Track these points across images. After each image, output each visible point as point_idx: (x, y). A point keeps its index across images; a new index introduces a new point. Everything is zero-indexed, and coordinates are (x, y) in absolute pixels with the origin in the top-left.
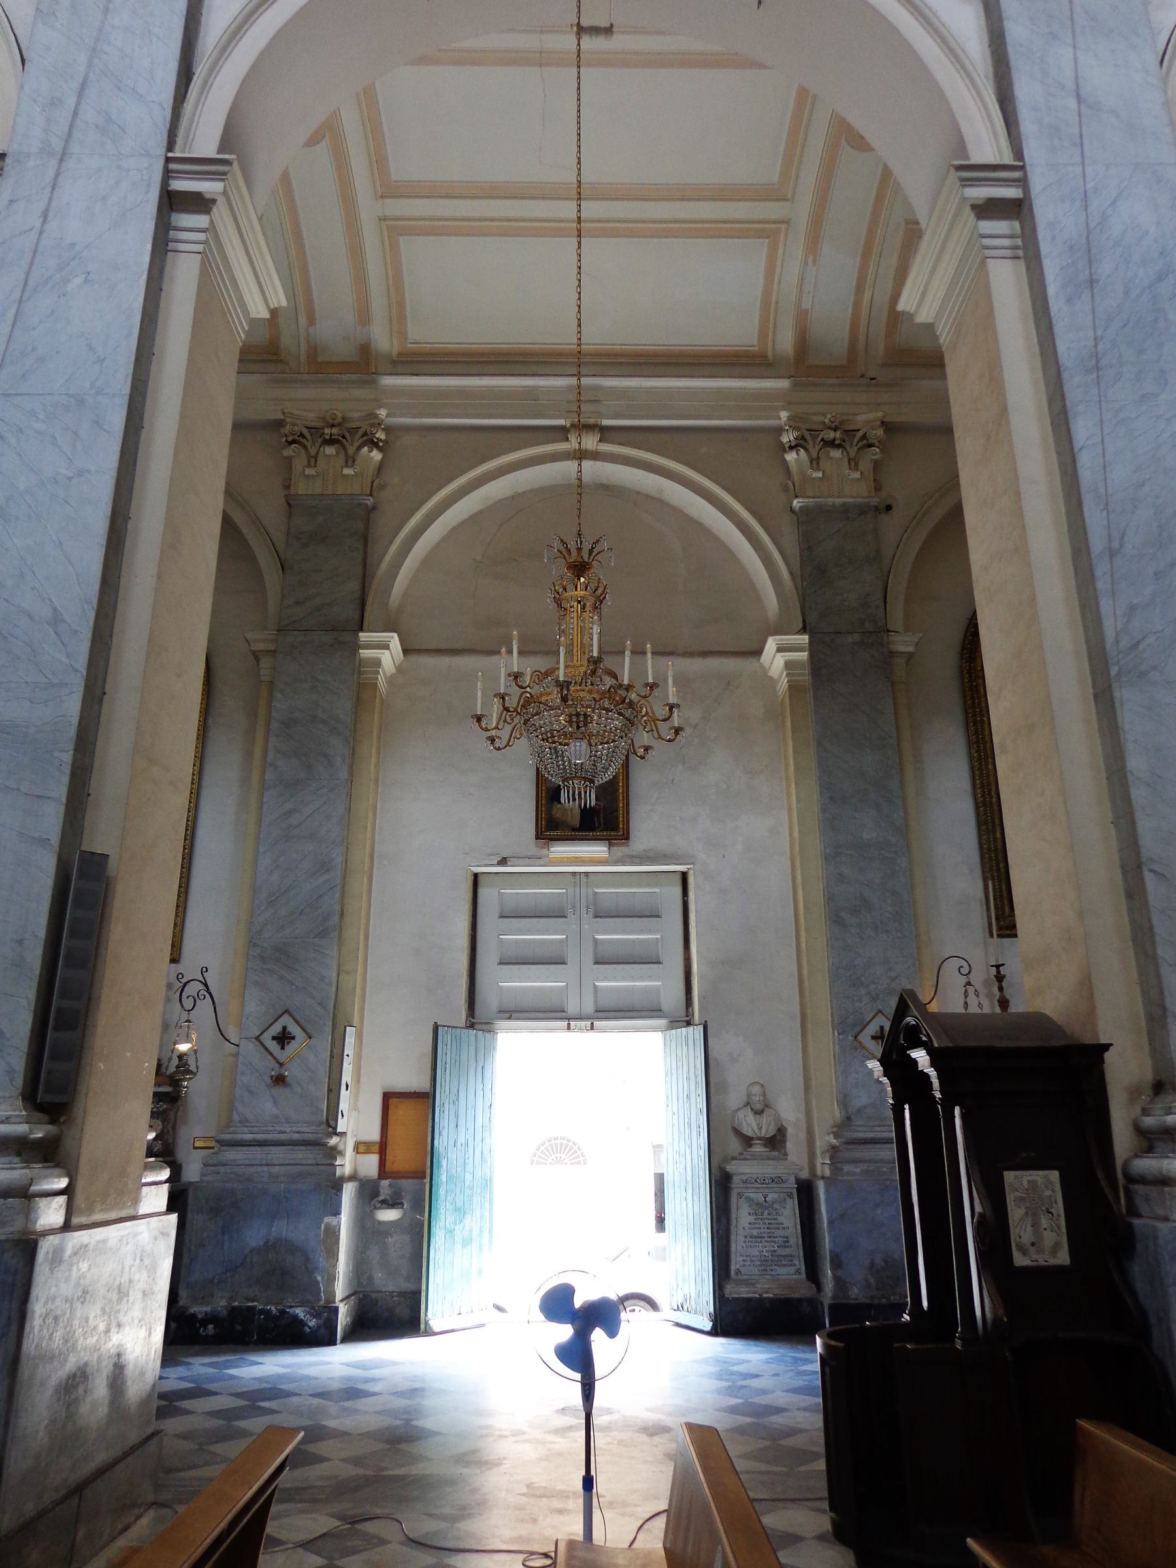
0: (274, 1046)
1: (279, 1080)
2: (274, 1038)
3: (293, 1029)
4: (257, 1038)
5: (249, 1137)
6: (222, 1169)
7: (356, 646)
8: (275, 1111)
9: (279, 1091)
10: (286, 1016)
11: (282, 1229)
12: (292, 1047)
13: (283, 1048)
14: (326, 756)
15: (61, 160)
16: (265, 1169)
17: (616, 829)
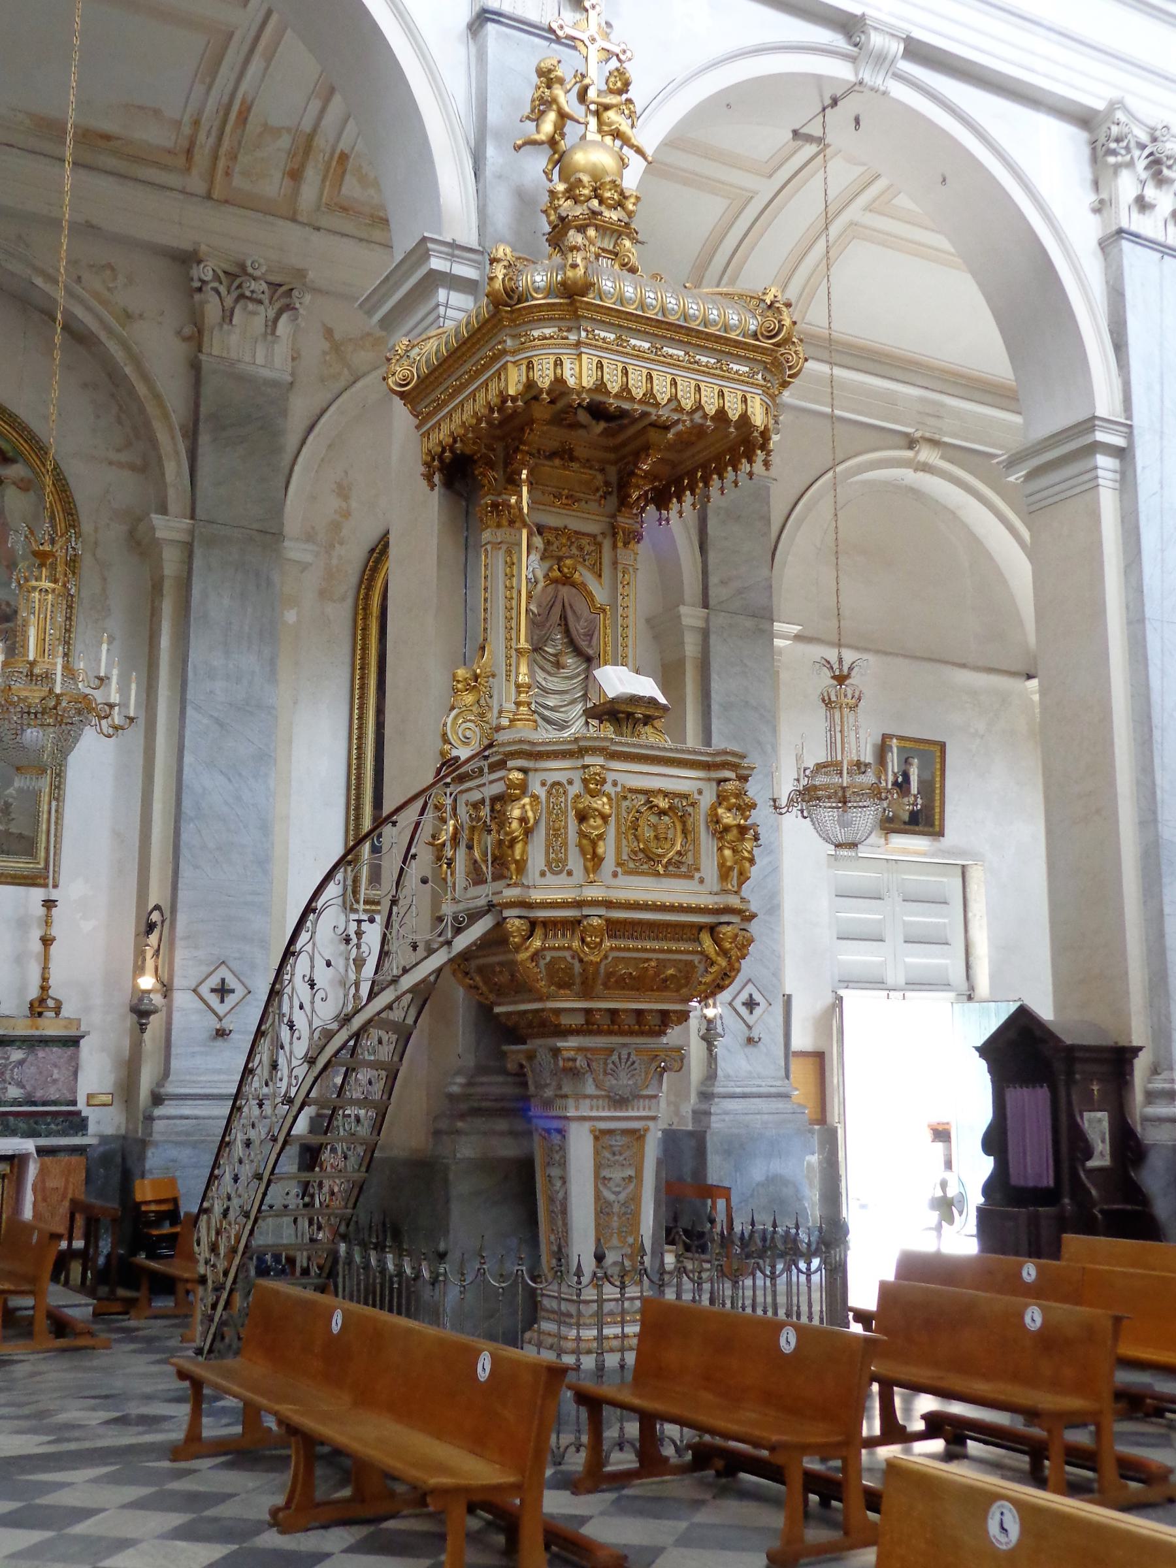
0: (743, 1011)
1: (750, 1041)
2: (744, 1004)
3: (757, 997)
4: (730, 1004)
5: (738, 1090)
6: (727, 1118)
7: (771, 636)
8: (749, 1068)
9: (750, 1050)
10: (750, 985)
11: (777, 1167)
12: (758, 1011)
13: (751, 1013)
14: (759, 743)
15: (1161, 438)
16: (758, 1117)
17: (932, 825)
